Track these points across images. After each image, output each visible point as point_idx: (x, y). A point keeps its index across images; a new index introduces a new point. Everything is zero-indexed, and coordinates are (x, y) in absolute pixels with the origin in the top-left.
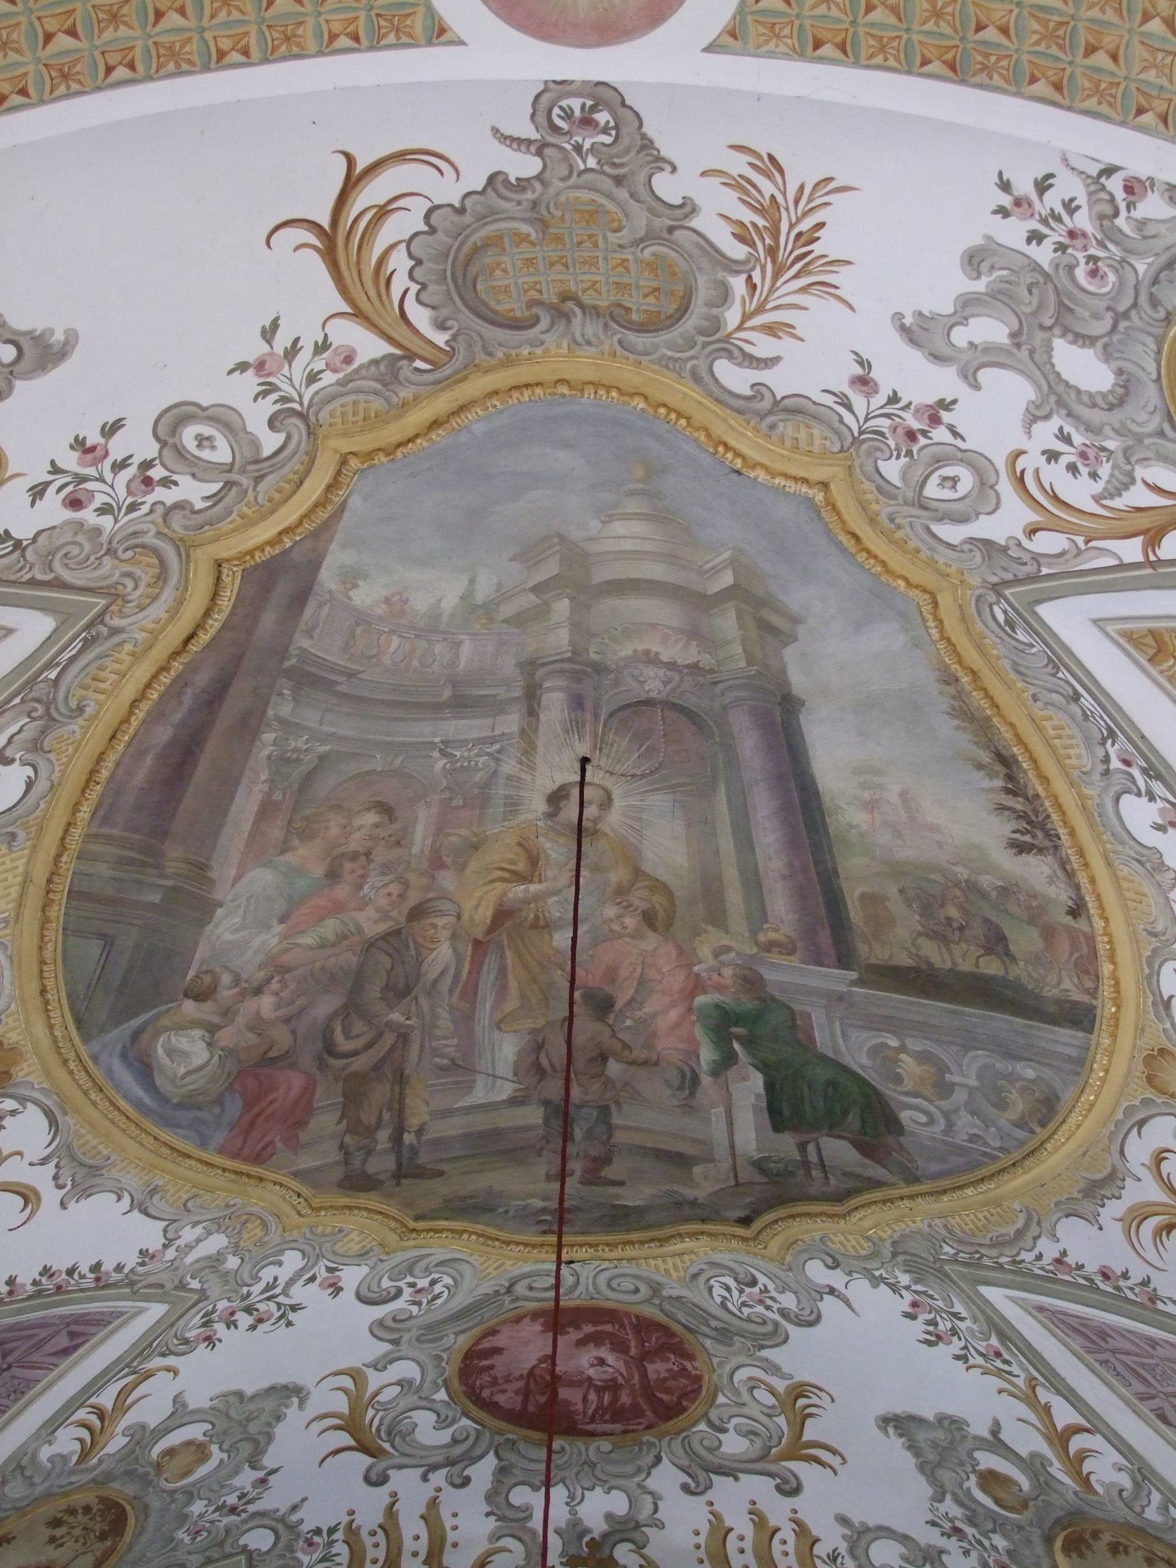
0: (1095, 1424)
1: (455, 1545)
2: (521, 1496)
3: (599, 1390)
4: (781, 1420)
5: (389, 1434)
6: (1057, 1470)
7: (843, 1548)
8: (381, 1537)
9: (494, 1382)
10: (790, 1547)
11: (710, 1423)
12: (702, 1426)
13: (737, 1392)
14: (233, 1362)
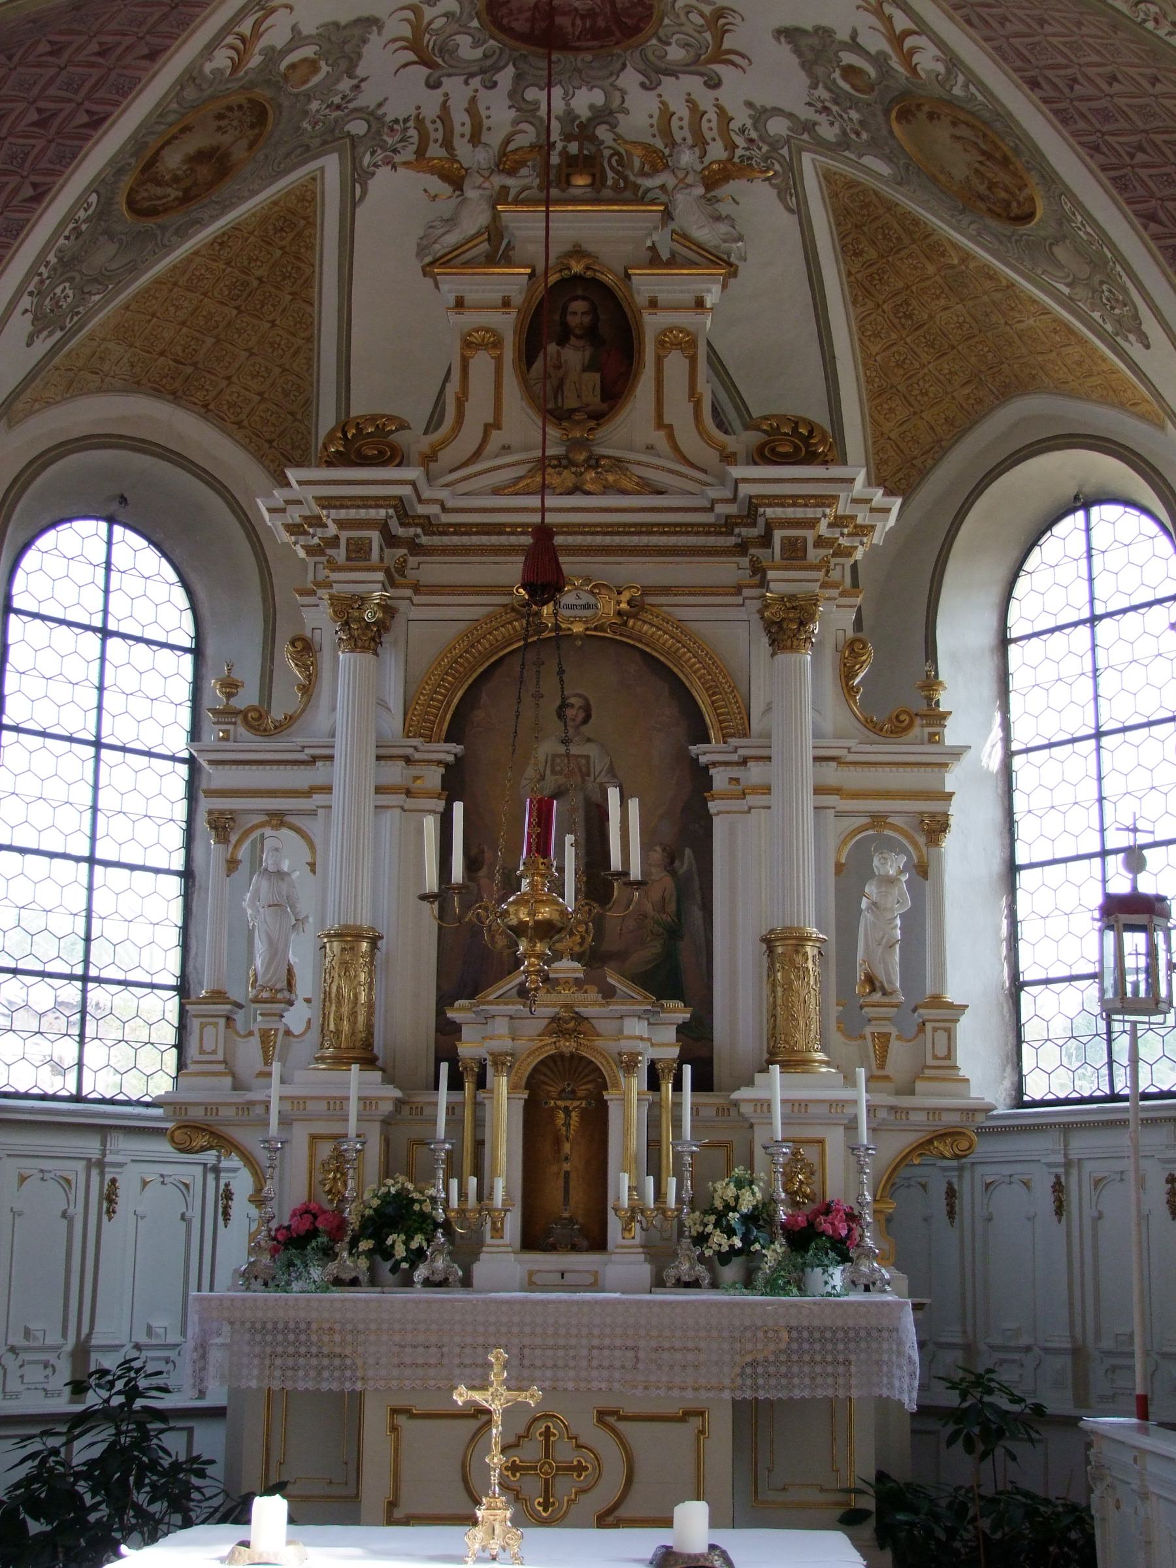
0: (923, 28)
1: (489, 129)
2: (532, 94)
3: (583, 17)
4: (708, 35)
5: (441, 51)
6: (895, 63)
7: (749, 123)
8: (439, 124)
9: (511, 12)
10: (714, 124)
11: (660, 40)
12: (654, 41)
13: (678, 16)
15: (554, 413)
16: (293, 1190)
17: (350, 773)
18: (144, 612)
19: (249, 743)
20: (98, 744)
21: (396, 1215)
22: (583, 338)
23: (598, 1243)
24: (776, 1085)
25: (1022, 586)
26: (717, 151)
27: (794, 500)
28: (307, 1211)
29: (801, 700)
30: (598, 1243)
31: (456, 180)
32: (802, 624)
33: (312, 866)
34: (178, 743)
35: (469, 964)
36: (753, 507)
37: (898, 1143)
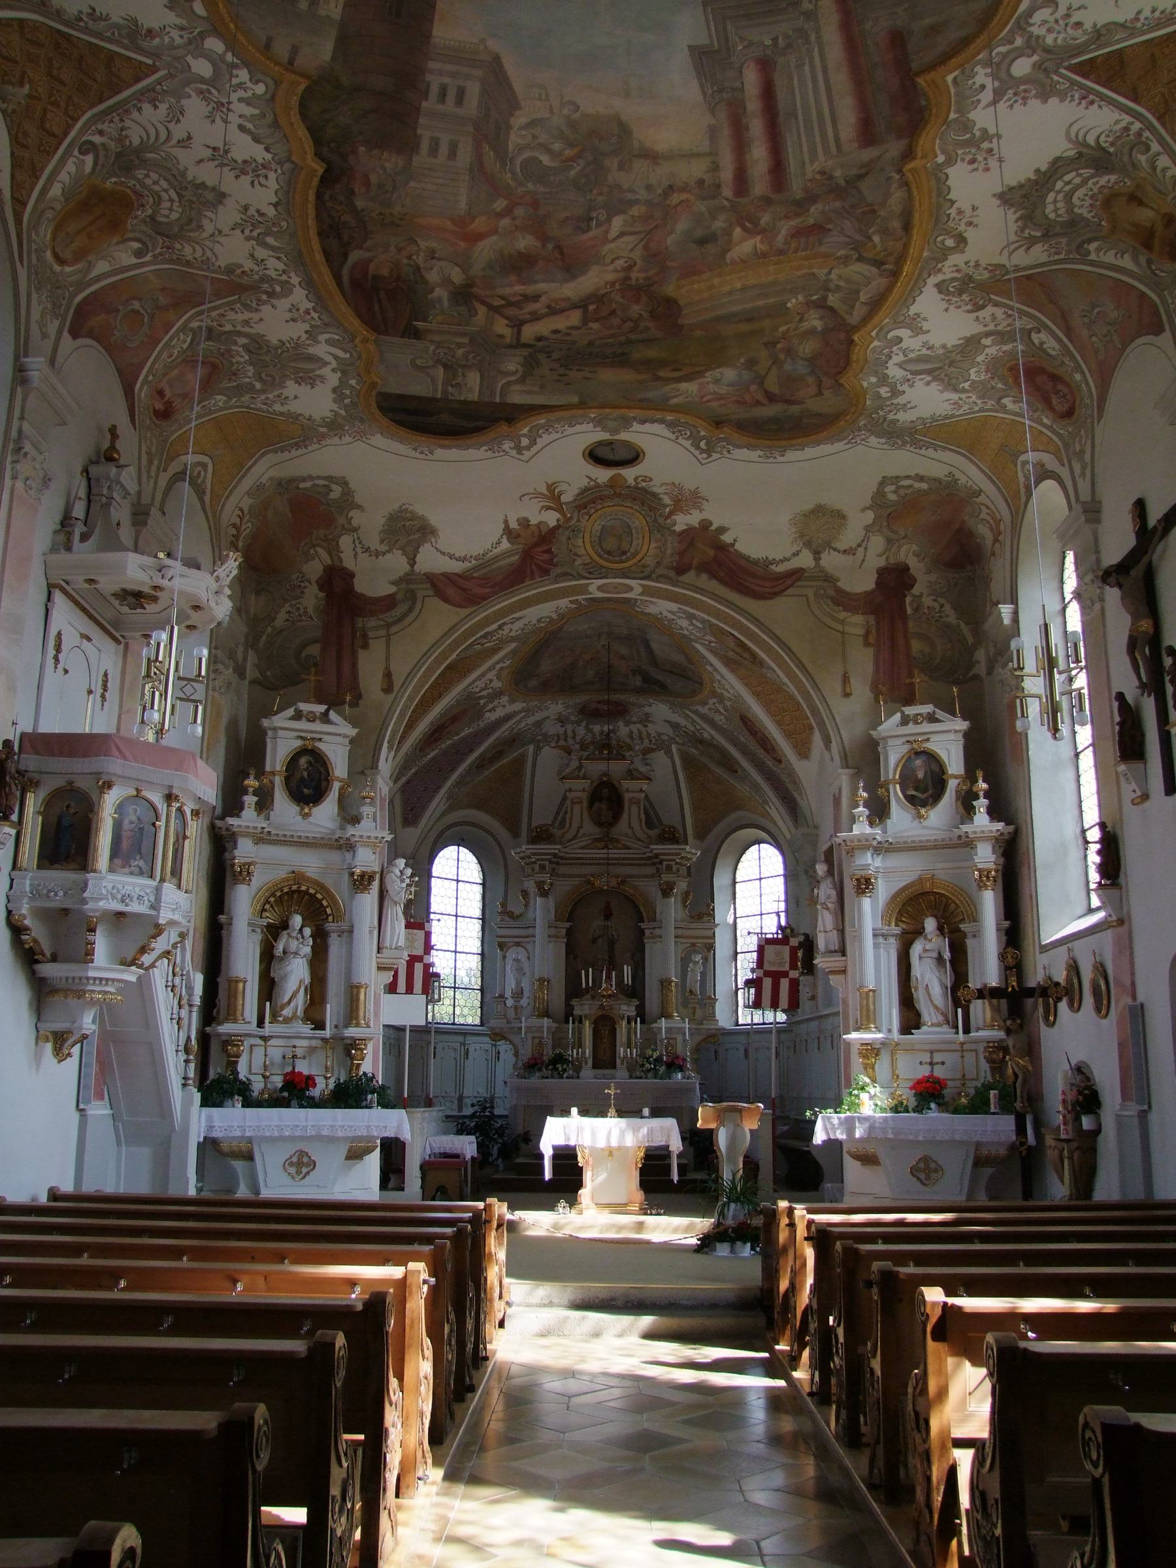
14: (538, 716)
15: (600, 824)
16: (527, 1052)
17: (540, 932)
19: (509, 922)
20: (456, 916)
21: (559, 1059)
22: (607, 800)
23: (613, 1066)
25: (740, 866)
27: (669, 854)
28: (533, 1058)
29: (672, 911)
30: (614, 1066)
31: (569, 752)
32: (671, 890)
33: (529, 958)
35: (574, 990)
36: (656, 856)
37: (698, 1038)
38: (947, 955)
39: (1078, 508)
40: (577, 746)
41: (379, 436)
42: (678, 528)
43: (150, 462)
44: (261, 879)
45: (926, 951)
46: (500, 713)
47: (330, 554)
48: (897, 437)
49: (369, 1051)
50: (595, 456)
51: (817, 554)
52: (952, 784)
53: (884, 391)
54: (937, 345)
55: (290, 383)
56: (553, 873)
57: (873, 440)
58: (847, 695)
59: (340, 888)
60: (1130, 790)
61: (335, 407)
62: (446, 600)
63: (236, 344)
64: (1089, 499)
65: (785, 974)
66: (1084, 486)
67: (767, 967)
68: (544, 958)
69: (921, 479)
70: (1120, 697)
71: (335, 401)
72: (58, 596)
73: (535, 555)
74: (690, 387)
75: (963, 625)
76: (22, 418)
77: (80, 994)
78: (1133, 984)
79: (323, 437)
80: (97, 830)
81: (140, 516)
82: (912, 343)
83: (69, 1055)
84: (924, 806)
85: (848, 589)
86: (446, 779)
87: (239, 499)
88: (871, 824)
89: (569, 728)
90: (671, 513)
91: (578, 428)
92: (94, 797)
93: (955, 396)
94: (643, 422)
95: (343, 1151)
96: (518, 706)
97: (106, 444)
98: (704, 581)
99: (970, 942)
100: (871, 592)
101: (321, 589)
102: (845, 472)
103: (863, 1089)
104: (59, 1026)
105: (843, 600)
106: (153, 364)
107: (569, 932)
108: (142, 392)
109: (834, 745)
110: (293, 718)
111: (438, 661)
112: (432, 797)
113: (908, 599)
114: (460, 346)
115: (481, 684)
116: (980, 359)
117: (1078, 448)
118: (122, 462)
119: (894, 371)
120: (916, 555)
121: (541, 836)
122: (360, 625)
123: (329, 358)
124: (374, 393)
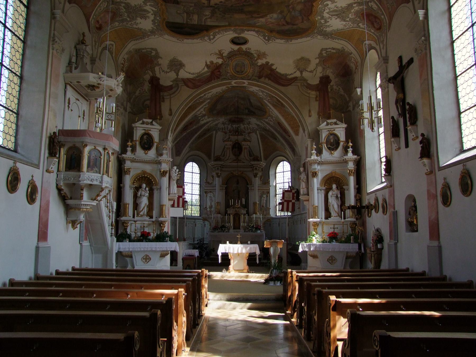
14: (216, 122)
16: (213, 225)
17: (217, 187)
18: (196, 170)
21: (223, 227)
22: (237, 148)
23: (239, 229)
24: (254, 216)
26: (249, 131)
28: (216, 226)
29: (257, 182)
30: (239, 229)
31: (226, 133)
34: (198, 183)
35: (227, 206)
36: (252, 165)
37: (264, 220)
38: (339, 196)
39: (381, 59)
40: (228, 132)
41: (166, 35)
42: (259, 64)
43: (96, 44)
44: (133, 173)
45: (333, 194)
46: (205, 121)
47: (152, 72)
48: (327, 36)
49: (166, 225)
50: (233, 41)
51: (301, 72)
52: (341, 144)
53: (323, 21)
54: (339, 6)
55: (139, 19)
56: (221, 170)
57: (319, 37)
58: (310, 116)
59: (157, 176)
60: (395, 146)
61: (152, 26)
62: (188, 87)
63: (121, 6)
64: (385, 56)
65: (291, 201)
66: (383, 52)
67: (285, 199)
68: (218, 196)
69: (334, 49)
70: (393, 118)
71: (153, 24)
72: (68, 87)
73: (215, 73)
74: (263, 20)
75: (345, 95)
76: (54, 30)
77: (79, 209)
78: (394, 205)
79: (149, 35)
80: (83, 160)
81: (93, 61)
82: (331, 6)
83: (77, 227)
84: (333, 150)
85: (311, 83)
86: (189, 142)
87: (124, 55)
88: (317, 156)
89: (226, 126)
90: (257, 60)
91: (228, 33)
92: (82, 149)
93: (344, 23)
94: (248, 31)
95: (159, 255)
96: (210, 119)
97: (82, 38)
98: (267, 81)
99: (346, 192)
100: (318, 84)
101: (150, 84)
102: (310, 47)
103: (313, 236)
104: (74, 219)
105: (310, 87)
106: (95, 13)
107: (226, 188)
108: (92, 21)
109: (306, 132)
110: (142, 124)
111: (186, 106)
112: (184, 147)
113: (329, 87)
114: (191, 6)
115: (199, 113)
116: (352, 11)
117: (382, 39)
118: (87, 44)
119: (326, 15)
120: (331, 73)
121: (218, 159)
122: (162, 95)
123: (150, 10)
124: (165, 22)
